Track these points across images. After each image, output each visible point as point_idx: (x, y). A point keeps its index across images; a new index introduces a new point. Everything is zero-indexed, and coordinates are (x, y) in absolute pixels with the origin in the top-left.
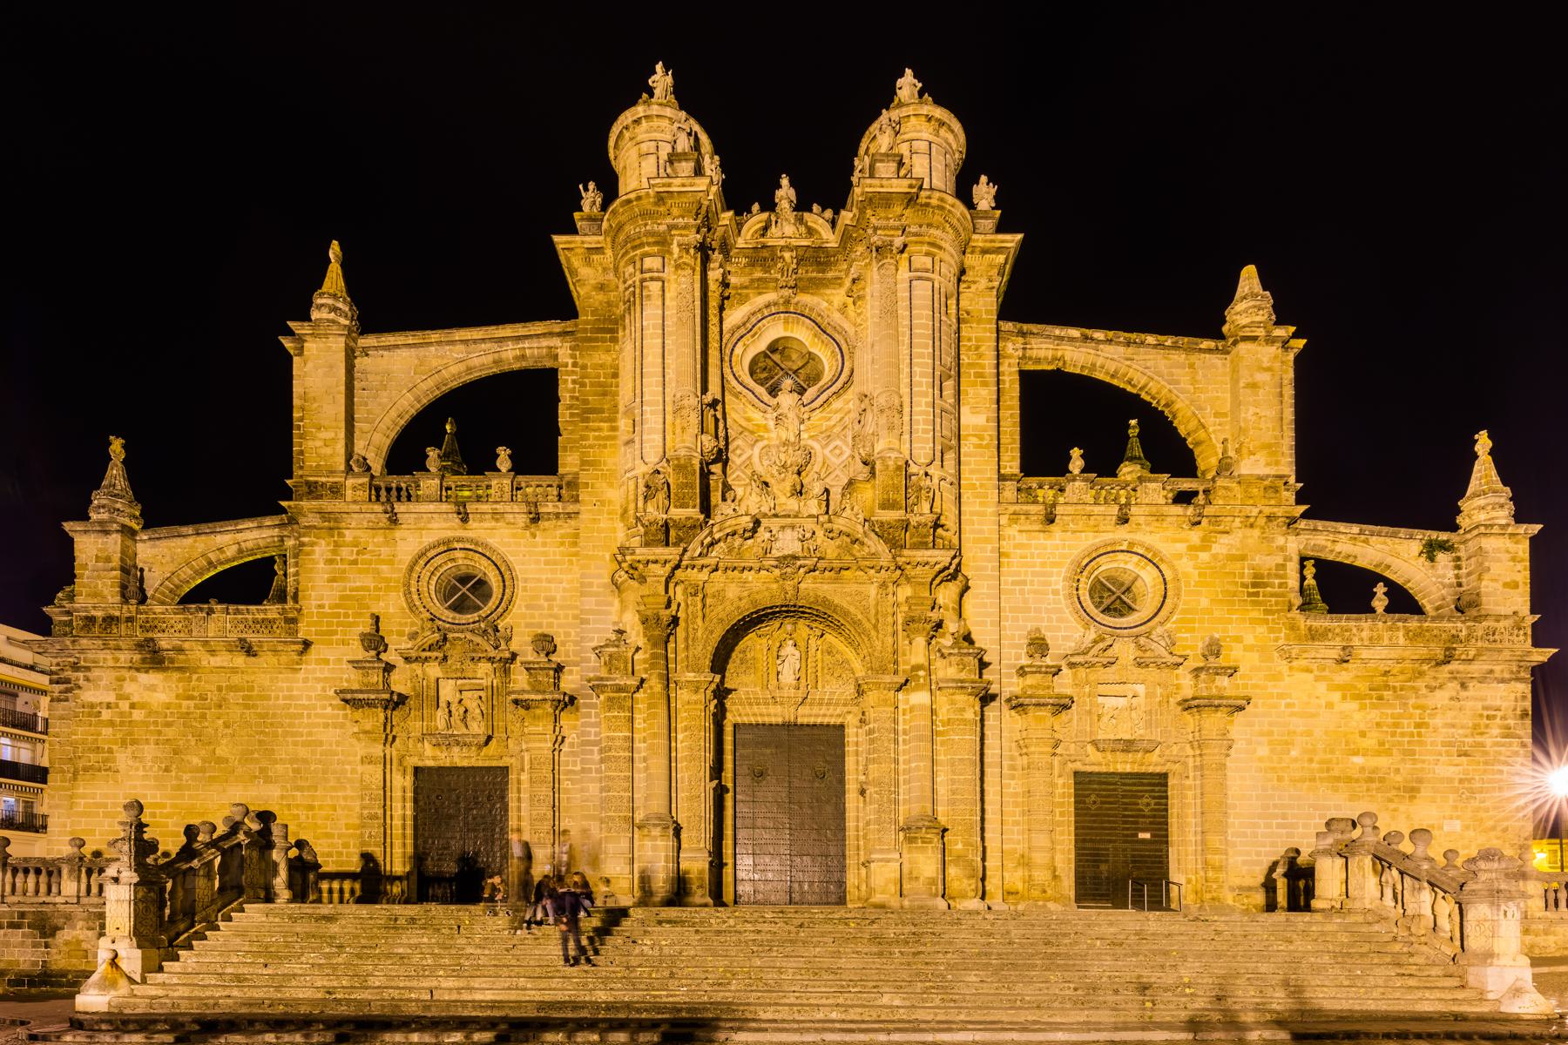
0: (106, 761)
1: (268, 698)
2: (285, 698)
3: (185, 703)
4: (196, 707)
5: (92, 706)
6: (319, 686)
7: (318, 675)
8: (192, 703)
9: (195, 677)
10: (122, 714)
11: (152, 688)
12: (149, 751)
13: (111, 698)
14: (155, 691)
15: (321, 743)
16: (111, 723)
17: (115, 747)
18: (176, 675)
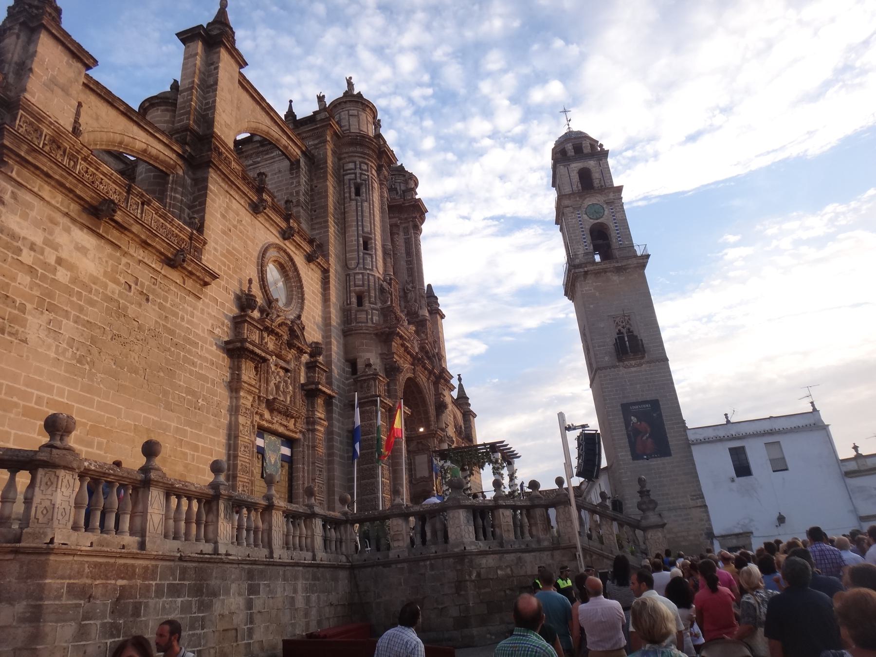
0: (13, 320)
1: (175, 315)
2: (189, 322)
3: (111, 285)
4: (120, 293)
5: (14, 236)
6: (211, 322)
7: (210, 311)
8: (117, 289)
9: (124, 260)
10: (45, 265)
11: (82, 250)
12: (68, 328)
13: (38, 238)
14: (85, 254)
15: (204, 378)
16: (31, 270)
17: (29, 306)
18: (108, 249)
